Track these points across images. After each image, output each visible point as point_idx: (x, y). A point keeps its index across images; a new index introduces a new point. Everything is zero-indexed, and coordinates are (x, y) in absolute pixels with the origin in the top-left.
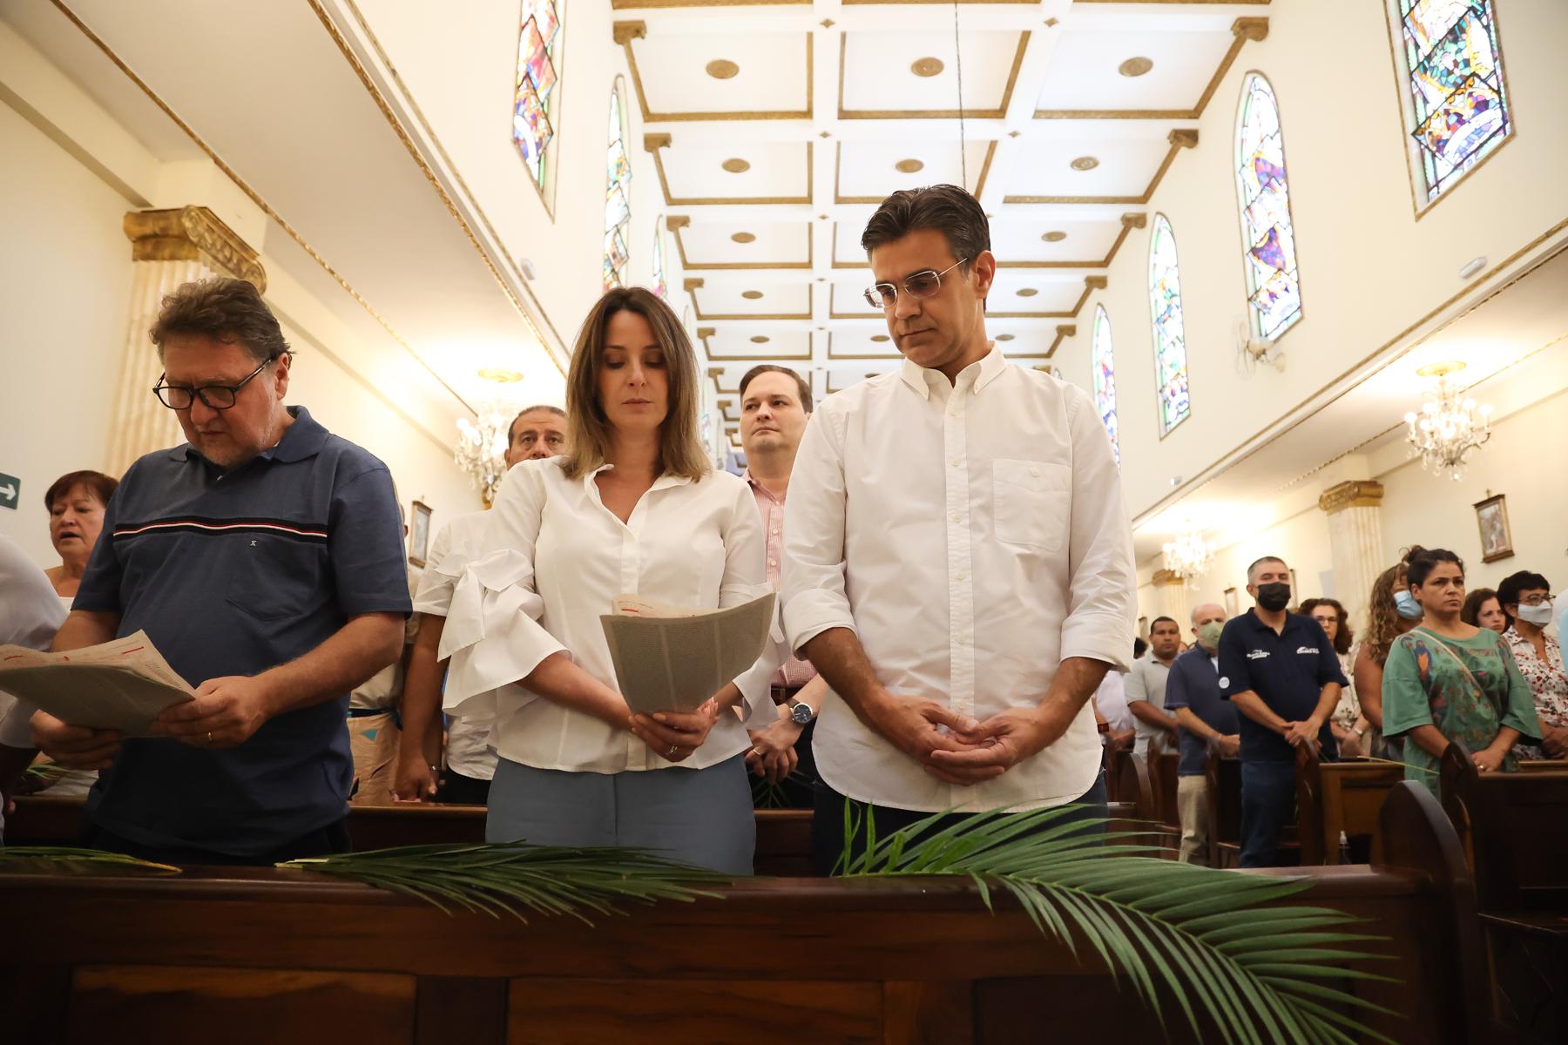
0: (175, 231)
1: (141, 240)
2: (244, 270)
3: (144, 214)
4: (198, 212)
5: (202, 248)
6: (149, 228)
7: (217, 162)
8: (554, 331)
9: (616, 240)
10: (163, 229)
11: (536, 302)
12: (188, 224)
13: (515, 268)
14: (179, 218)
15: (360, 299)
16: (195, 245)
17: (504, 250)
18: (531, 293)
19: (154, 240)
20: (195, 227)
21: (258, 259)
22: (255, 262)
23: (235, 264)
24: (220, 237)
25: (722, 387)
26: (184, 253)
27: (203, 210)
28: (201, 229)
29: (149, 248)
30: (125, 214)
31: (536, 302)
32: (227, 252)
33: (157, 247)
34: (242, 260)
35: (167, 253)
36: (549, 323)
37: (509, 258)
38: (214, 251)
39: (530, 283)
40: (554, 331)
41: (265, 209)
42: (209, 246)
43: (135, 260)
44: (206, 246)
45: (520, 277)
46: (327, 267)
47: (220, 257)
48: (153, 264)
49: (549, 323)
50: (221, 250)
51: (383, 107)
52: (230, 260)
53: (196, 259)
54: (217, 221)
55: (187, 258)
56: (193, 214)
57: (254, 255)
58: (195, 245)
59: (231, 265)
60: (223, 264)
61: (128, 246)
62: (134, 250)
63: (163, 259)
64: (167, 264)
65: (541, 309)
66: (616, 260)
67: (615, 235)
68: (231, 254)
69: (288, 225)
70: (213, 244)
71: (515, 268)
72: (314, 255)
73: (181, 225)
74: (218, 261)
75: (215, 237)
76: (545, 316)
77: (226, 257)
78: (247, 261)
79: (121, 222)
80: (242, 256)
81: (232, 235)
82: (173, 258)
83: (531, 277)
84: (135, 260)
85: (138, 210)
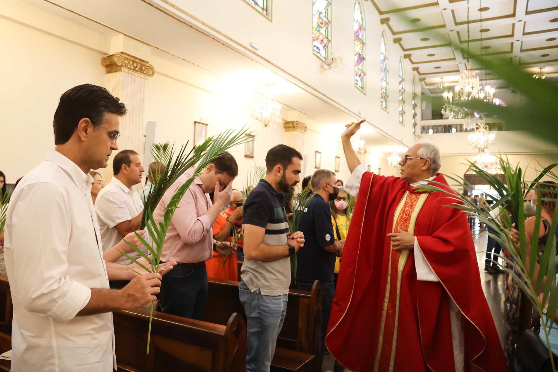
0: (114, 63)
1: (107, 66)
2: (143, 69)
3: (108, 57)
4: (120, 54)
5: (123, 66)
6: (107, 63)
7: (125, 35)
8: (276, 66)
9: (321, 17)
10: (111, 62)
11: (262, 58)
12: (116, 59)
13: (245, 48)
14: (113, 57)
15: (200, 66)
16: (122, 66)
17: (236, 43)
18: (258, 55)
19: (110, 66)
20: (119, 59)
21: (149, 63)
22: (148, 65)
23: (139, 68)
24: (131, 60)
25: (414, 61)
26: (118, 69)
27: (122, 53)
28: (122, 60)
29: (109, 69)
30: (101, 59)
31: (262, 58)
32: (135, 65)
33: (112, 68)
34: (141, 67)
35: (114, 70)
36: (272, 64)
37: (241, 45)
38: (129, 66)
39: (257, 52)
40: (276, 66)
41: (148, 45)
42: (127, 65)
43: (106, 73)
44: (125, 65)
45: (250, 51)
46: (181, 58)
47: (132, 67)
48: (110, 74)
49: (272, 64)
50: (133, 64)
51: (157, 8)
52: (136, 67)
53: (121, 71)
54: (128, 55)
55: (119, 71)
56: (118, 56)
57: (148, 62)
58: (122, 66)
59: (137, 69)
60: (134, 70)
61: (104, 69)
62: (106, 70)
63: (113, 72)
64: (115, 74)
65: (266, 60)
66: (323, 24)
67: (319, 15)
68: (137, 65)
69: (160, 48)
70: (129, 63)
71: (245, 48)
72: (174, 56)
73: (114, 61)
74: (131, 69)
75: (129, 60)
76: (269, 62)
77: (134, 66)
78: (144, 65)
79: (100, 62)
80: (142, 64)
81: (136, 58)
82: (116, 71)
83: (256, 49)
84: (106, 73)
85: (106, 56)
